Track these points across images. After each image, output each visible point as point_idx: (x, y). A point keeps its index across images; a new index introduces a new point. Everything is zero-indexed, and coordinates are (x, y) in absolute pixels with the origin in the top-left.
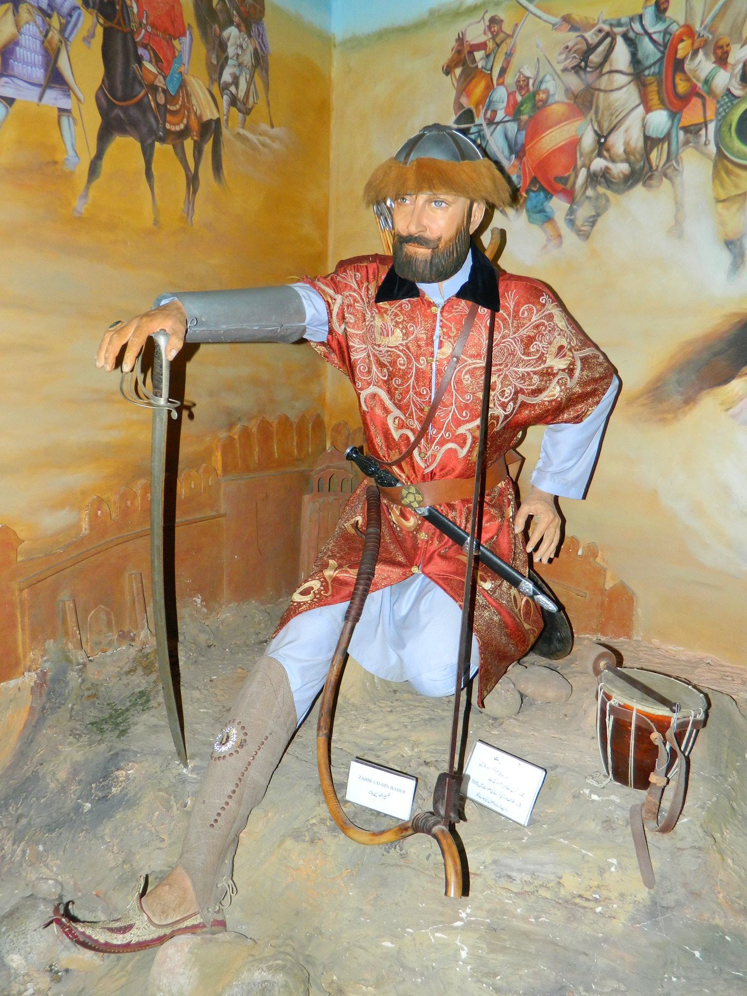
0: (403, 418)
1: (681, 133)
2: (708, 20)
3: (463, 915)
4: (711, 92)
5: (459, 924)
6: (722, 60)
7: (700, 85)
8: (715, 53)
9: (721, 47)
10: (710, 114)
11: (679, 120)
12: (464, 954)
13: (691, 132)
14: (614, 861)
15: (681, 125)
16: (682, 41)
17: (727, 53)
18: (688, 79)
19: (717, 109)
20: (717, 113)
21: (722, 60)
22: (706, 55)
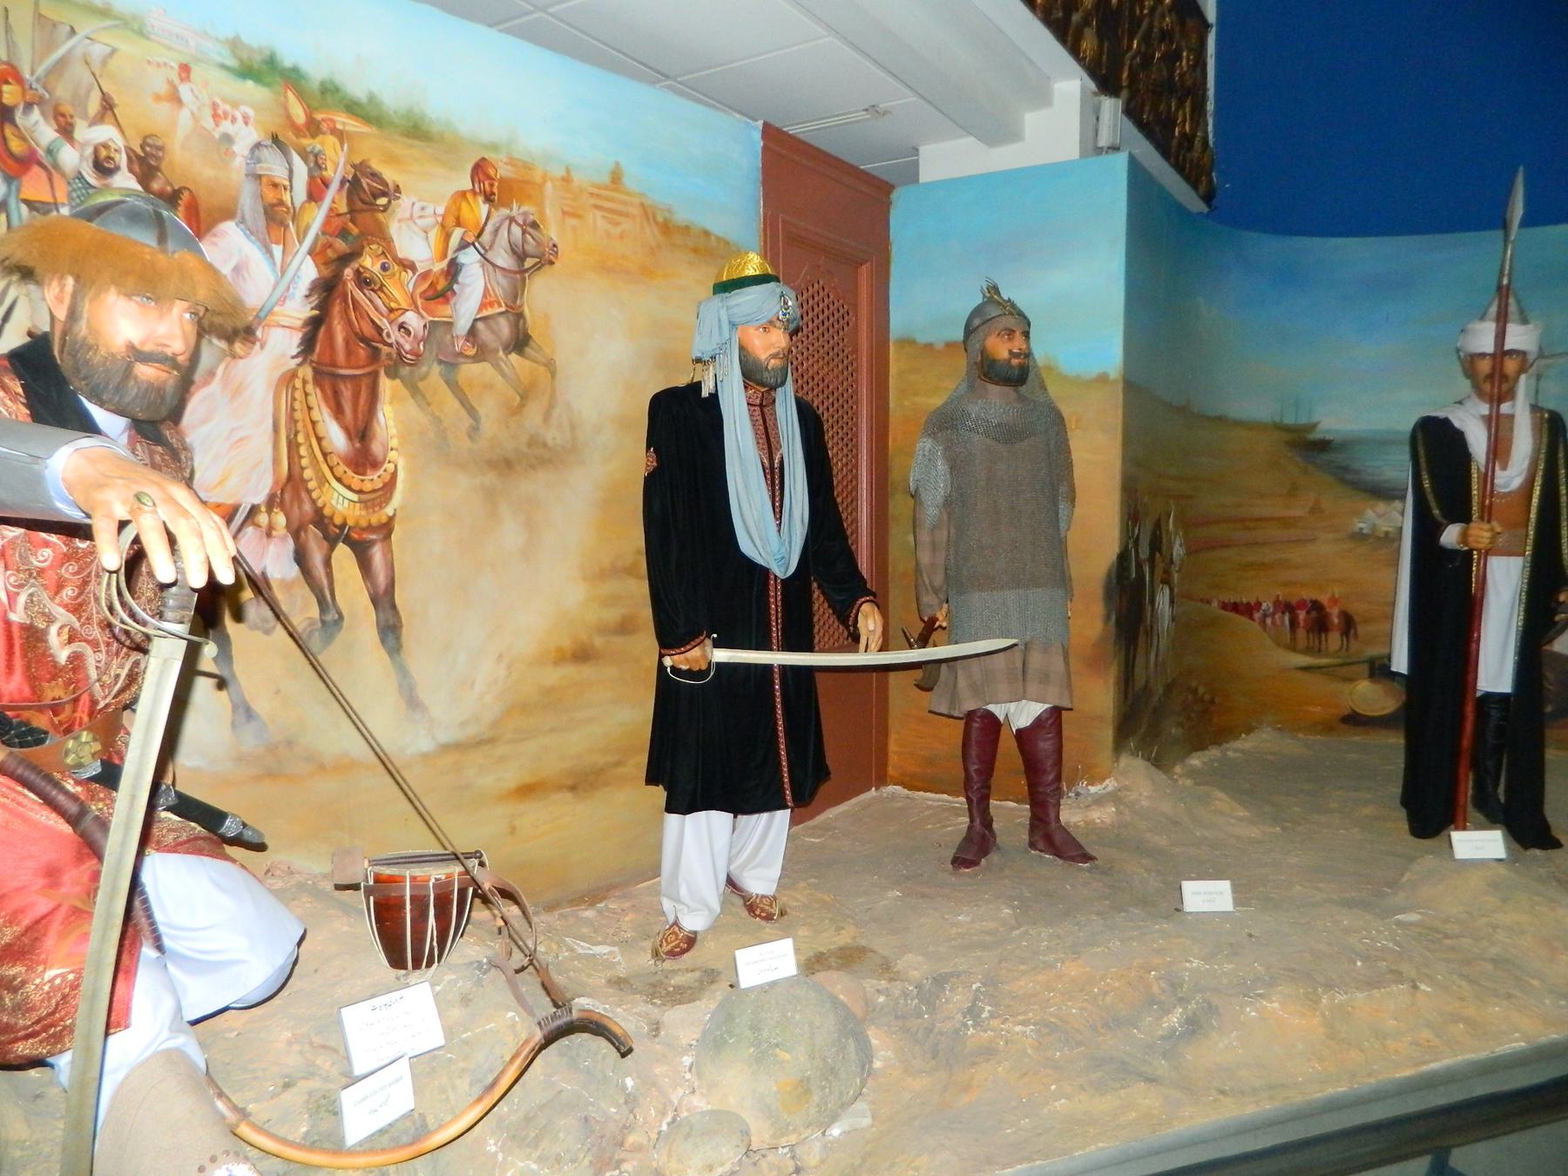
0: (77, 625)
1: (24, 208)
2: (40, 71)
3: (493, 1149)
4: (56, 166)
5: (500, 1157)
6: (66, 131)
7: (41, 152)
8: (55, 118)
9: (63, 115)
10: (61, 196)
11: (18, 191)
12: (534, 1166)
13: (37, 210)
14: (511, 1014)
15: (22, 196)
16: (7, 82)
17: (72, 125)
18: (23, 139)
19: (69, 193)
20: (70, 198)
21: (66, 131)
22: (43, 114)
